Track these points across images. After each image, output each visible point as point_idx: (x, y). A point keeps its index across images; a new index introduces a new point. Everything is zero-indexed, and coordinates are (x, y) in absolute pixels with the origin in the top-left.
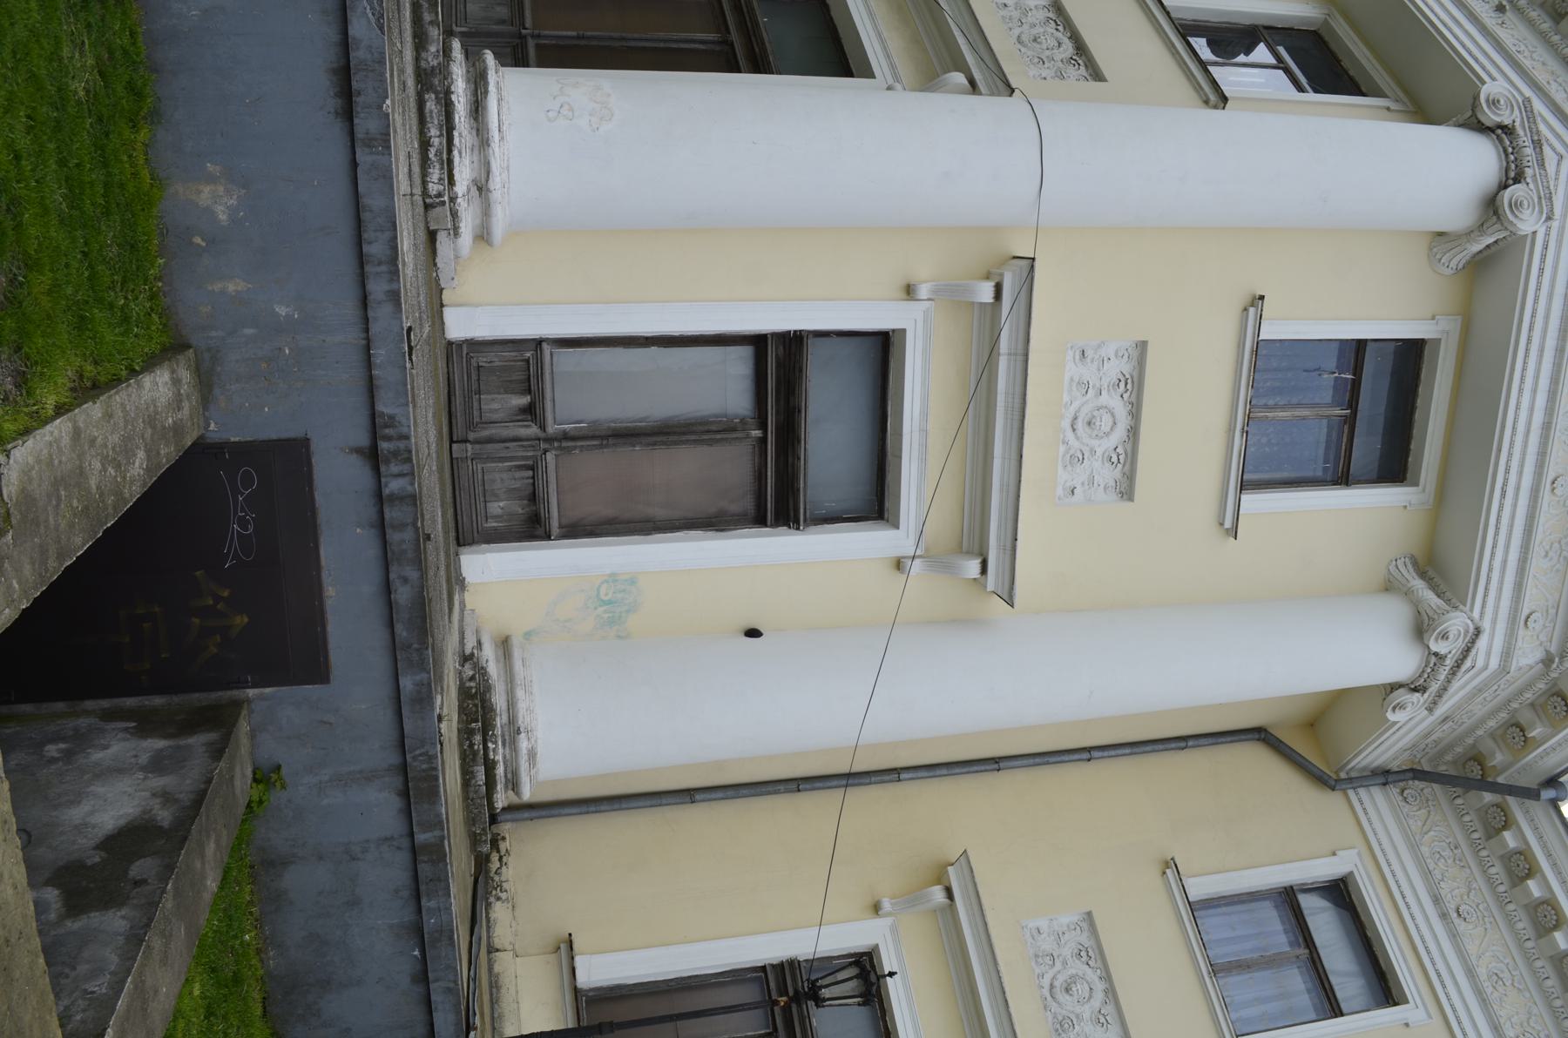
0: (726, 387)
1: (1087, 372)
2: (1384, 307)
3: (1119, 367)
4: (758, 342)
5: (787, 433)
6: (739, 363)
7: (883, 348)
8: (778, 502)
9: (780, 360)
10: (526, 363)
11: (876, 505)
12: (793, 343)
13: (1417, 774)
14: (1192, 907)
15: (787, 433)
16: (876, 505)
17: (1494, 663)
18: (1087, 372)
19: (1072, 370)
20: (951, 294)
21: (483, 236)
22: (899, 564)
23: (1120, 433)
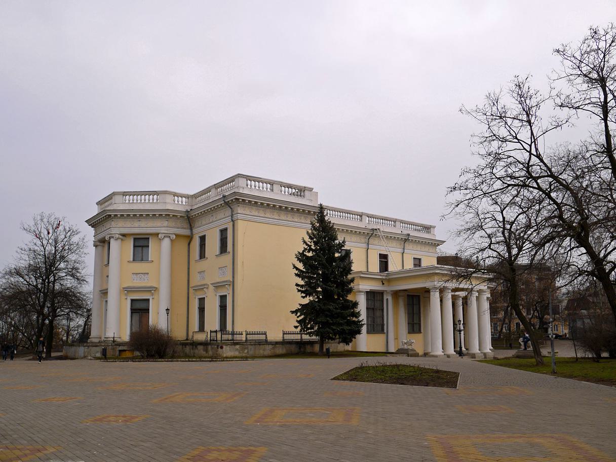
0: (136, 316)
1: (135, 279)
2: (130, 244)
3: (135, 276)
4: (132, 313)
5: (140, 310)
6: (134, 314)
7: (132, 300)
8: (147, 310)
9: (133, 311)
10: (132, 335)
11: (149, 300)
12: (132, 309)
13: (191, 225)
14: (200, 259)
15: (140, 310)
16: (149, 300)
17: (166, 228)
18: (135, 279)
19: (135, 281)
20: (126, 295)
21: (120, 338)
22: (153, 298)
23: (142, 275)
